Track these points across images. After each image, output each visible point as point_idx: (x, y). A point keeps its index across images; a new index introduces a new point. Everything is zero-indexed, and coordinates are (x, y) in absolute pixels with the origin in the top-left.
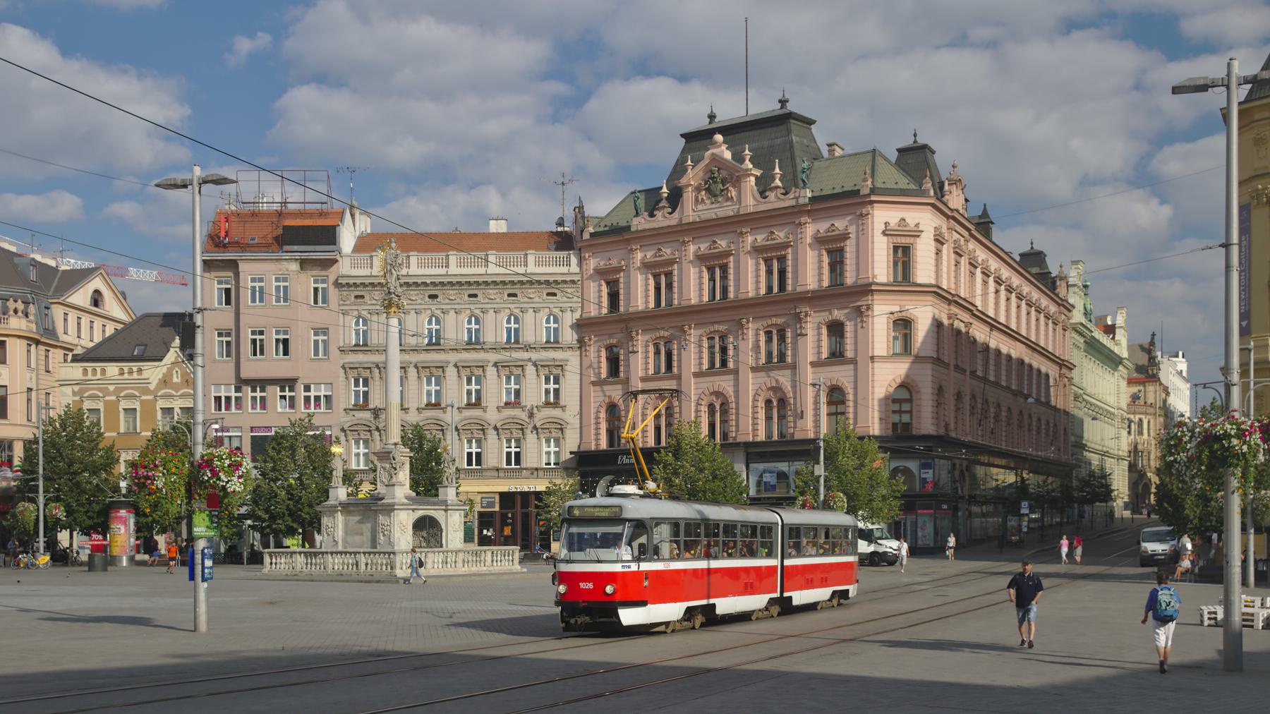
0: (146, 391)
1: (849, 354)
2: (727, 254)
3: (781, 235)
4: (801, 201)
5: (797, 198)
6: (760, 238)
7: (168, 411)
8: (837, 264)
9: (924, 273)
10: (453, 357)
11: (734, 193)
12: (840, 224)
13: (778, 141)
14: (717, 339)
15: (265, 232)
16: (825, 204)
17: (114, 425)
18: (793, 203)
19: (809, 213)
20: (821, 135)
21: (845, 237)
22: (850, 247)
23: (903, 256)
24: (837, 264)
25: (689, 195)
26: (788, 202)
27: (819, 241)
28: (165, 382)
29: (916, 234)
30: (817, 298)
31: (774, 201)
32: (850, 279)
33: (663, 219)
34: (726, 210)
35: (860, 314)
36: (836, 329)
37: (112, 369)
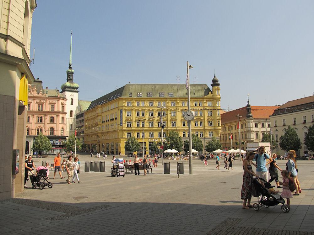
1: (55, 122)
2: (44, 103)
4: (46, 96)
5: (46, 96)
6: (38, 101)
11: (33, 93)
12: (54, 101)
13: (39, 85)
14: (40, 118)
16: (50, 97)
18: (45, 96)
19: (48, 98)
20: (44, 85)
21: (55, 103)
22: (44, 105)
26: (44, 96)
27: (50, 103)
30: (48, 112)
31: (41, 95)
32: (56, 110)
35: (57, 116)
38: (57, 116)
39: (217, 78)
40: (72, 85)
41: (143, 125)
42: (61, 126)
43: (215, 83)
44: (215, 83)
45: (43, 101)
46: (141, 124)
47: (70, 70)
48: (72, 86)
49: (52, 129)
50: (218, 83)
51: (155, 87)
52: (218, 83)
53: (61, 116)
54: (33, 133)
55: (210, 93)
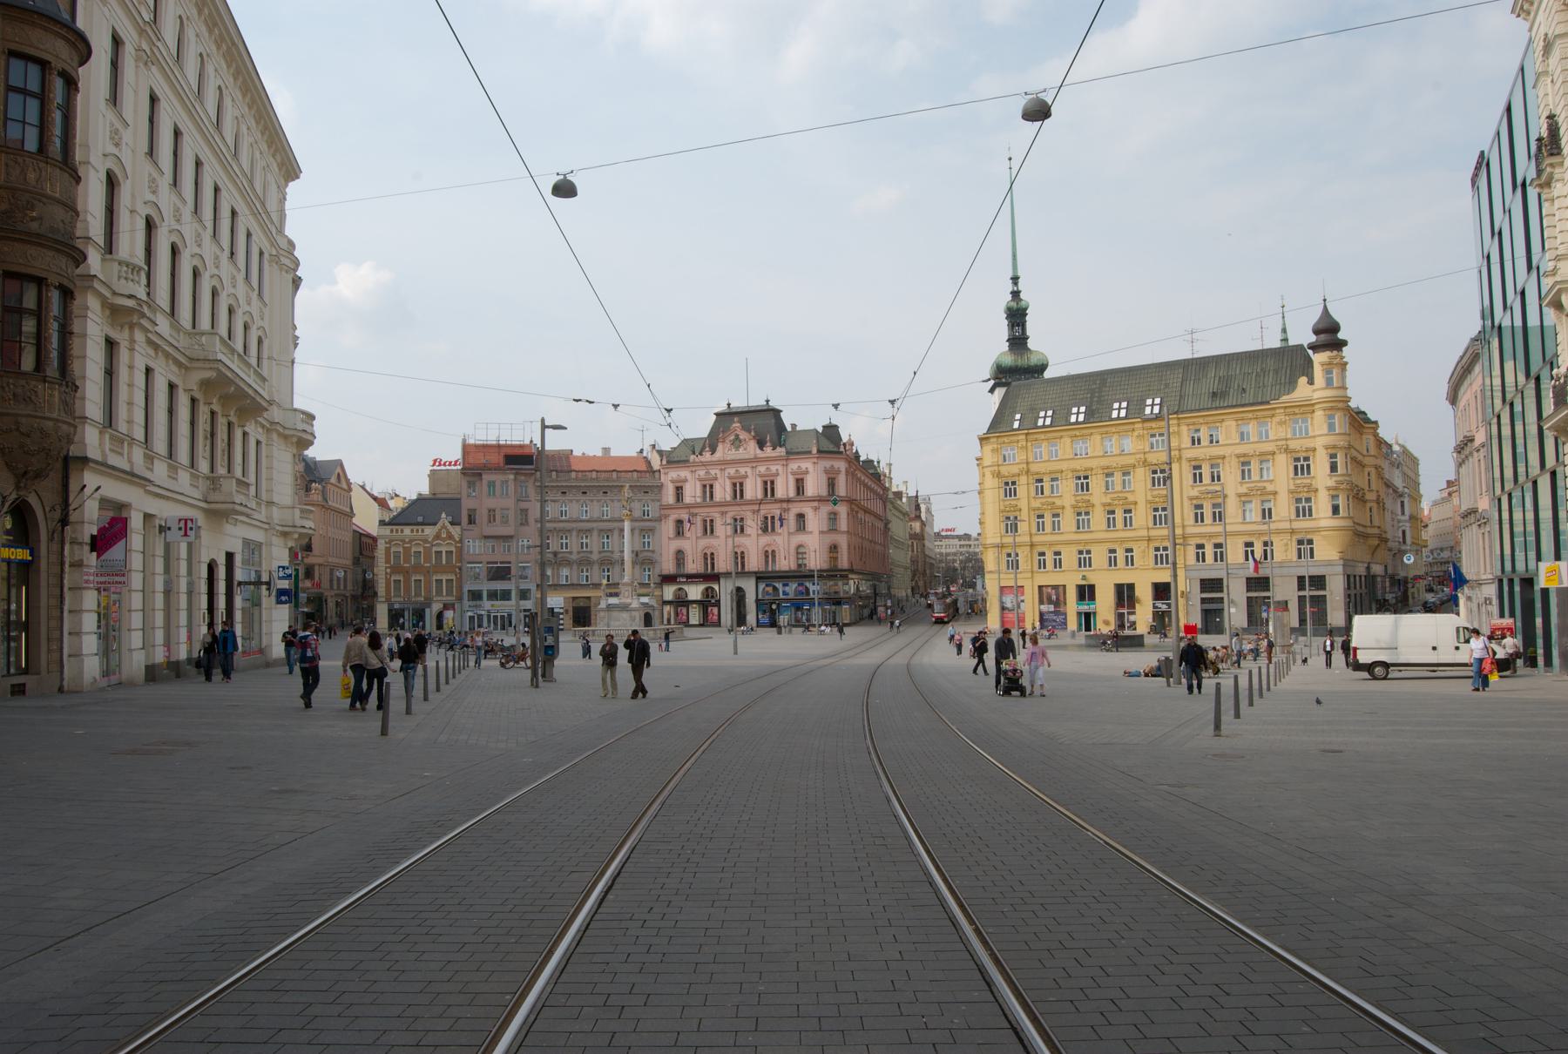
0: (426, 541)
3: (774, 468)
7: (439, 553)
8: (800, 485)
9: (842, 490)
10: (594, 525)
15: (498, 459)
17: (407, 560)
20: (787, 420)
23: (832, 484)
24: (800, 485)
25: (720, 447)
28: (438, 537)
29: (838, 472)
33: (707, 456)
34: (741, 453)
36: (801, 516)
37: (407, 530)
38: (816, 509)
39: (1336, 315)
40: (1022, 362)
41: (1056, 526)
42: (830, 539)
43: (1329, 335)
44: (1329, 335)
45: (774, 468)
46: (1048, 519)
47: (1014, 304)
48: (1020, 363)
49: (800, 551)
50: (1341, 336)
51: (1104, 382)
52: (1341, 336)
53: (826, 509)
54: (754, 563)
55: (1303, 380)
